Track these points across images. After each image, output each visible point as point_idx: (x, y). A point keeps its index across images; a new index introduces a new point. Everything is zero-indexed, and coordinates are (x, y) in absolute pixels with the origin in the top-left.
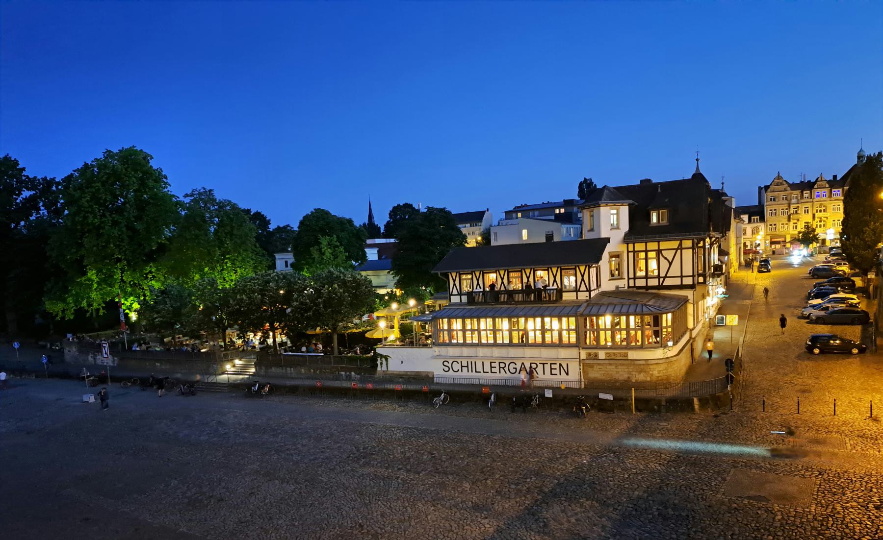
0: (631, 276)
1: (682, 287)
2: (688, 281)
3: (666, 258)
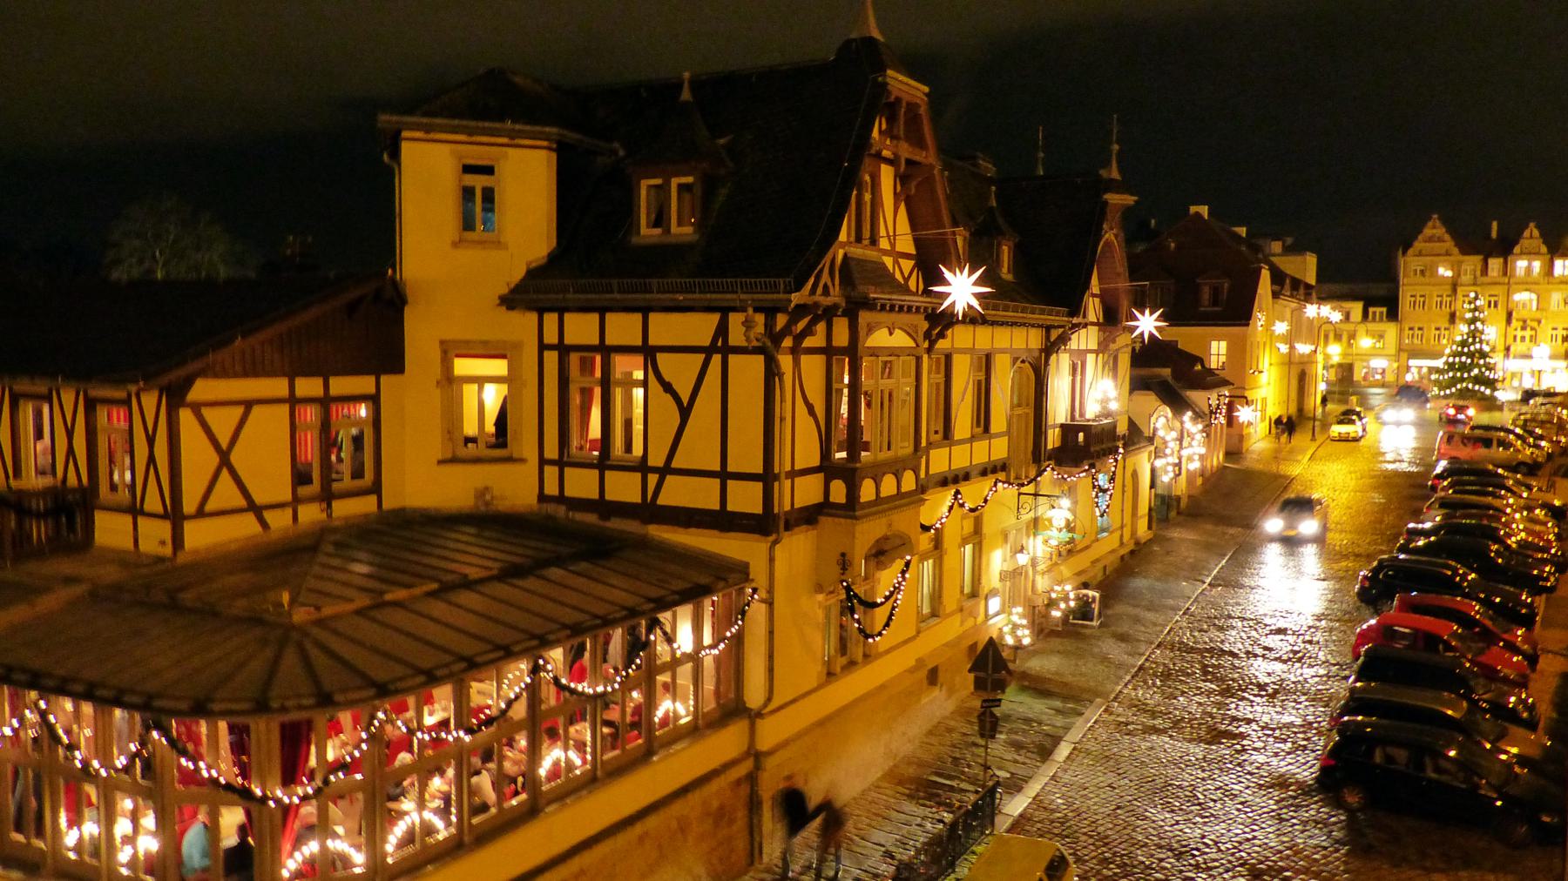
0: (552, 452)
1: (723, 520)
2: (746, 498)
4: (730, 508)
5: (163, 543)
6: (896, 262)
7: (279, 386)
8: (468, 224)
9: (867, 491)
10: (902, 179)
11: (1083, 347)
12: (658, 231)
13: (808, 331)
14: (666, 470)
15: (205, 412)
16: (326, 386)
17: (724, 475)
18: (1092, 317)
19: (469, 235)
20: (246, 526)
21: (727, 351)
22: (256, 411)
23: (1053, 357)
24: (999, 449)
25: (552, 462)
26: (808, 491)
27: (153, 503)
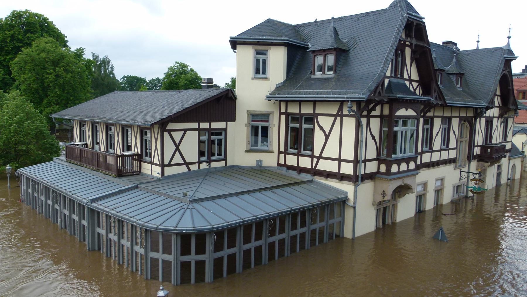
0: (282, 149)
2: (348, 169)
3: (321, 128)
4: (341, 172)
5: (158, 173)
6: (411, 83)
7: (195, 125)
8: (257, 71)
9: (394, 168)
10: (413, 52)
11: (492, 115)
12: (321, 73)
13: (374, 109)
14: (320, 157)
15: (172, 132)
16: (210, 125)
17: (340, 160)
18: (496, 104)
19: (258, 76)
20: (183, 169)
21: (342, 116)
22: (188, 132)
23: (478, 120)
24: (453, 154)
25: (282, 153)
26: (371, 167)
27: (156, 161)
